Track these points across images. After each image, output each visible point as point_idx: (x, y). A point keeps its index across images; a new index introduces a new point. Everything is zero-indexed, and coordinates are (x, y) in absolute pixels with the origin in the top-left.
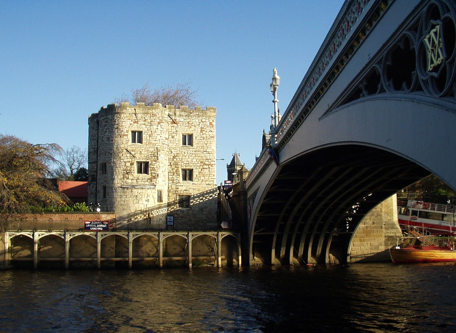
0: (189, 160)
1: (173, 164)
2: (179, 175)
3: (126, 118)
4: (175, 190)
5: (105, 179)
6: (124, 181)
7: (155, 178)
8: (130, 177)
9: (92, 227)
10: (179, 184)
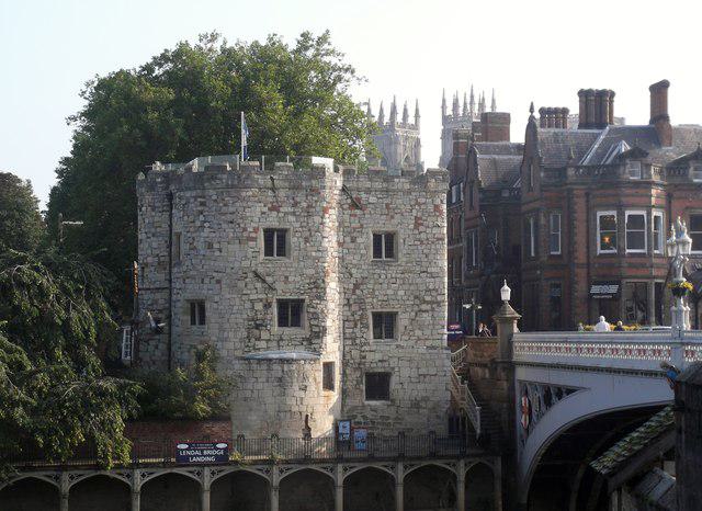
0: (390, 292)
1: (351, 301)
2: (368, 328)
7: (318, 337)
8: (265, 335)
9: (192, 457)
10: (367, 348)
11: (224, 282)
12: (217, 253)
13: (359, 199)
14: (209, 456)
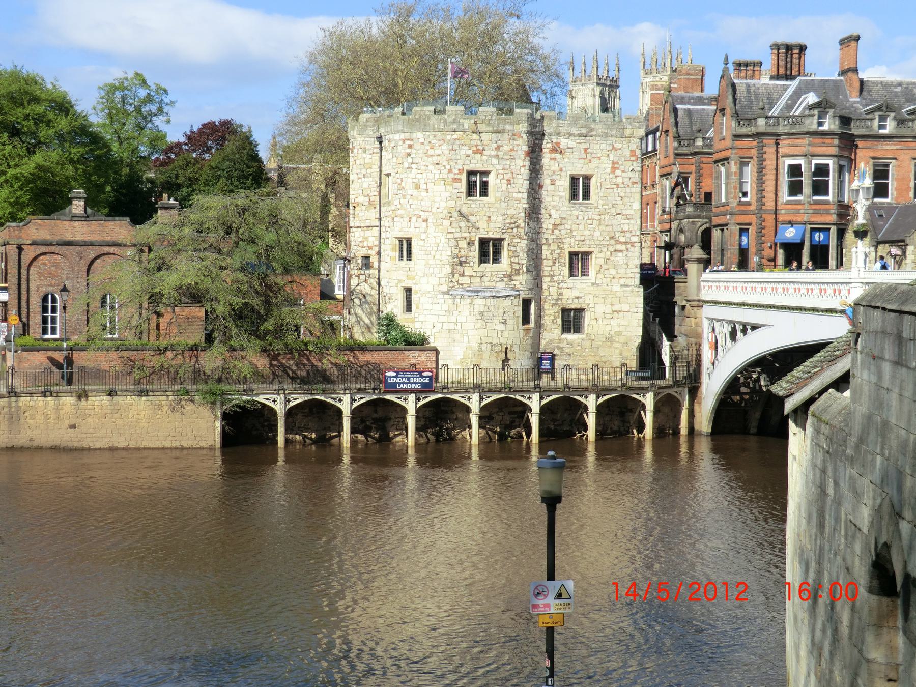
0: (587, 232)
3: (457, 142)
4: (556, 297)
5: (409, 273)
6: (454, 280)
7: (518, 274)
8: (468, 271)
11: (430, 221)
12: (424, 193)
13: (558, 144)
14: (415, 383)
